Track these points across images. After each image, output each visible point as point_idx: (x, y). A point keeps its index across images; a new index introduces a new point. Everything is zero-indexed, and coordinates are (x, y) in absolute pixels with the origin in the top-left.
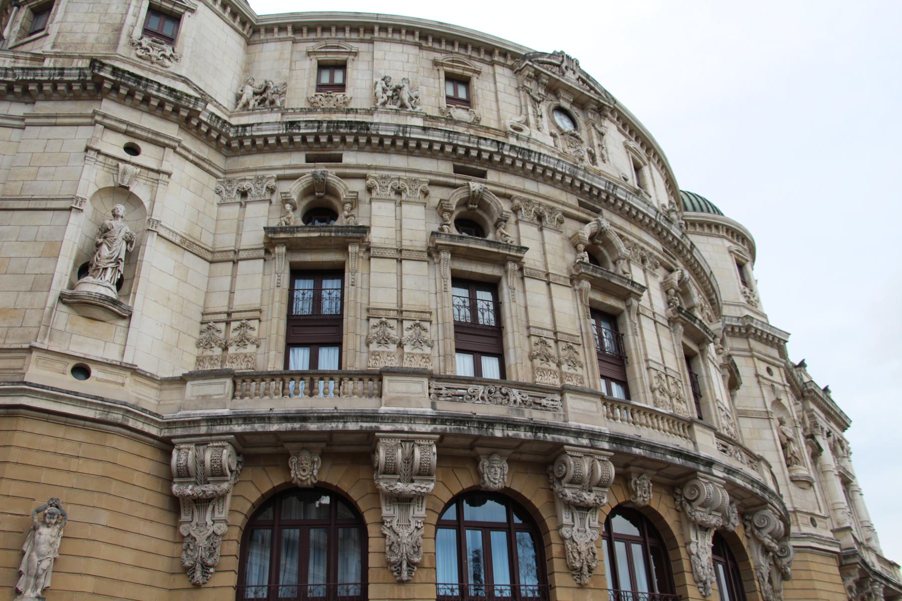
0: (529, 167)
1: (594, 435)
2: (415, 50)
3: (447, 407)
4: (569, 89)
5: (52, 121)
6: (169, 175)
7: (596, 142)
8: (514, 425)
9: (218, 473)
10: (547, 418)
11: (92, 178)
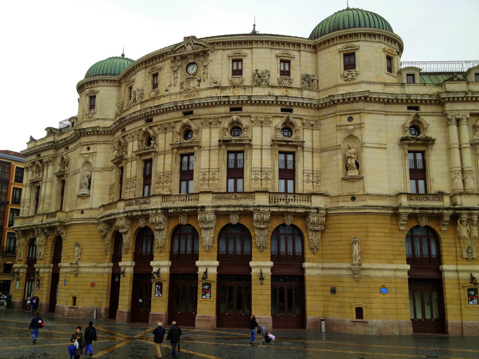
0: (161, 111)
1: (157, 209)
2: (143, 71)
3: (128, 208)
4: (190, 54)
6: (96, 152)
8: (137, 211)
11: (81, 161)
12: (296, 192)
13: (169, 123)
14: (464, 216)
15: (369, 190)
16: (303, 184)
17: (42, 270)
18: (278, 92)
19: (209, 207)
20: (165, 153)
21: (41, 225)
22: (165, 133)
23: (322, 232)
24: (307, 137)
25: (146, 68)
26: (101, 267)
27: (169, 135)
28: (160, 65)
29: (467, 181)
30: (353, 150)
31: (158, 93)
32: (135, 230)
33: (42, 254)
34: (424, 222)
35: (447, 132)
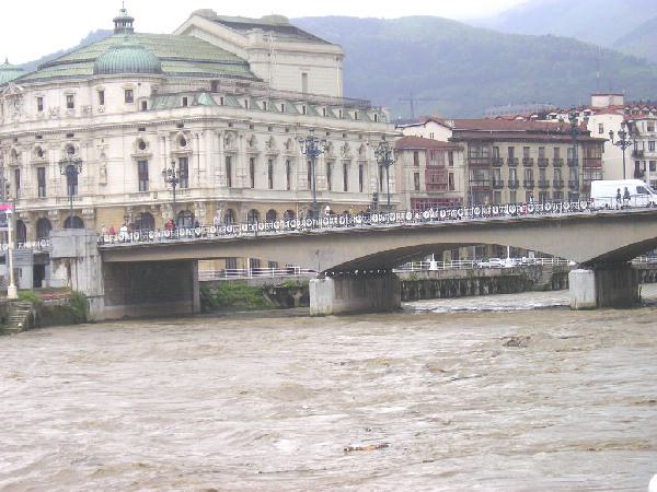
18: (64, 124)
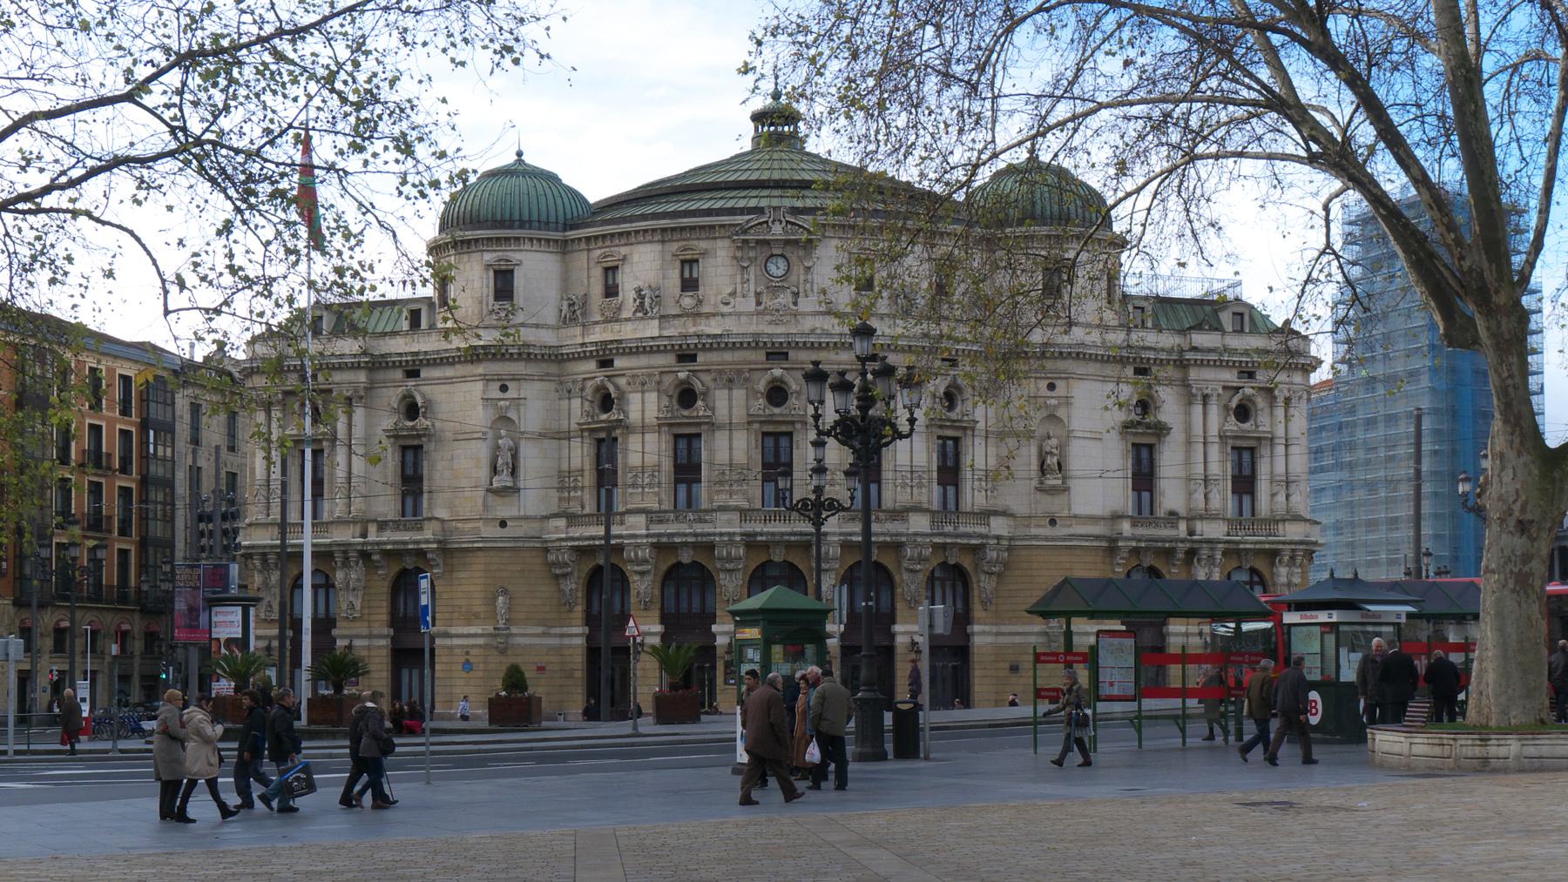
1: (729, 534)
2: (658, 247)
3: (657, 529)
5: (463, 379)
7: (802, 278)
8: (685, 535)
9: (566, 565)
10: (708, 528)
12: (963, 508)
13: (739, 372)
14: (1204, 553)
15: (1079, 509)
16: (973, 496)
17: (357, 643)
19: (834, 534)
20: (730, 427)
21: (364, 544)
22: (730, 389)
23: (999, 575)
24: (982, 414)
25: (663, 242)
26: (555, 635)
27: (739, 394)
28: (703, 245)
29: (1211, 496)
30: (1054, 442)
31: (700, 302)
32: (664, 567)
33: (358, 607)
34: (1148, 561)
35: (1188, 414)
